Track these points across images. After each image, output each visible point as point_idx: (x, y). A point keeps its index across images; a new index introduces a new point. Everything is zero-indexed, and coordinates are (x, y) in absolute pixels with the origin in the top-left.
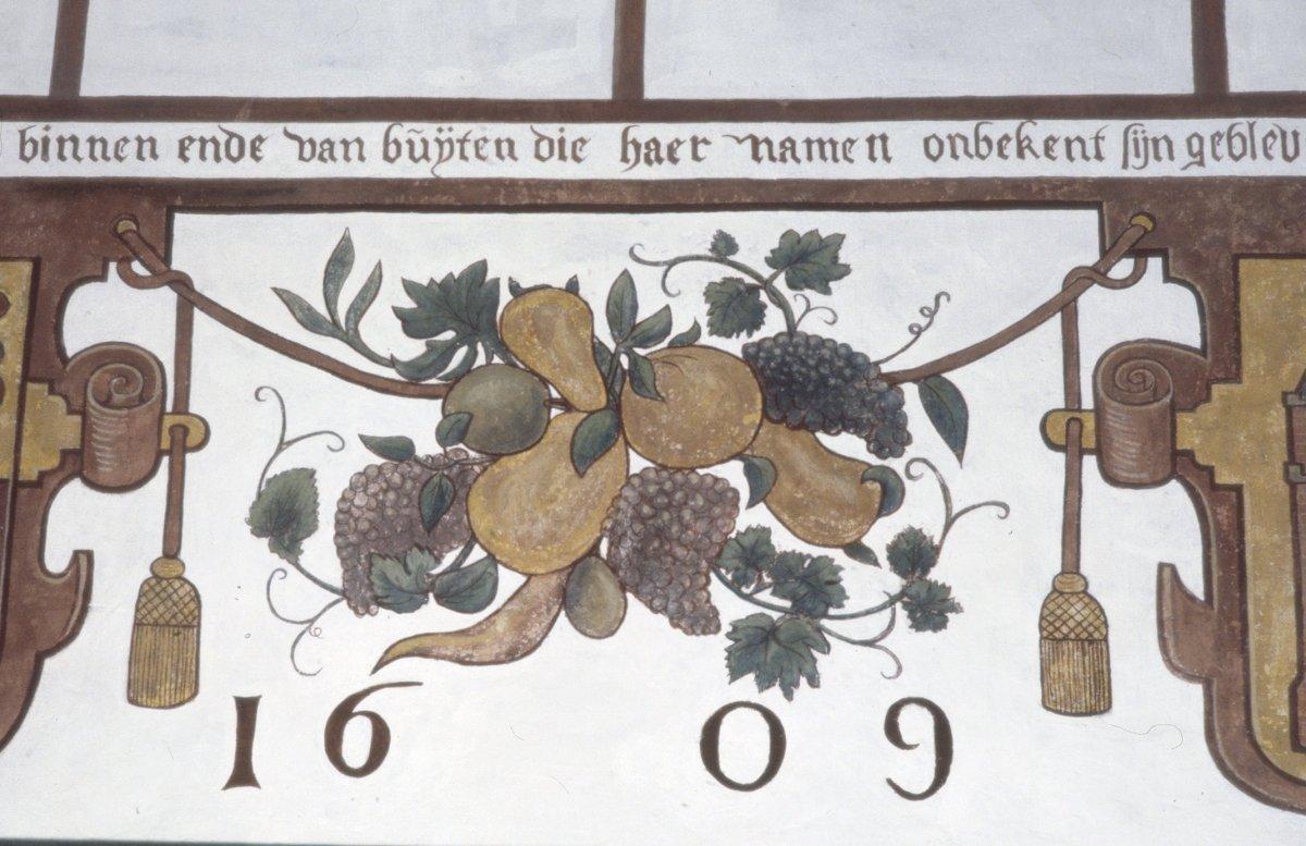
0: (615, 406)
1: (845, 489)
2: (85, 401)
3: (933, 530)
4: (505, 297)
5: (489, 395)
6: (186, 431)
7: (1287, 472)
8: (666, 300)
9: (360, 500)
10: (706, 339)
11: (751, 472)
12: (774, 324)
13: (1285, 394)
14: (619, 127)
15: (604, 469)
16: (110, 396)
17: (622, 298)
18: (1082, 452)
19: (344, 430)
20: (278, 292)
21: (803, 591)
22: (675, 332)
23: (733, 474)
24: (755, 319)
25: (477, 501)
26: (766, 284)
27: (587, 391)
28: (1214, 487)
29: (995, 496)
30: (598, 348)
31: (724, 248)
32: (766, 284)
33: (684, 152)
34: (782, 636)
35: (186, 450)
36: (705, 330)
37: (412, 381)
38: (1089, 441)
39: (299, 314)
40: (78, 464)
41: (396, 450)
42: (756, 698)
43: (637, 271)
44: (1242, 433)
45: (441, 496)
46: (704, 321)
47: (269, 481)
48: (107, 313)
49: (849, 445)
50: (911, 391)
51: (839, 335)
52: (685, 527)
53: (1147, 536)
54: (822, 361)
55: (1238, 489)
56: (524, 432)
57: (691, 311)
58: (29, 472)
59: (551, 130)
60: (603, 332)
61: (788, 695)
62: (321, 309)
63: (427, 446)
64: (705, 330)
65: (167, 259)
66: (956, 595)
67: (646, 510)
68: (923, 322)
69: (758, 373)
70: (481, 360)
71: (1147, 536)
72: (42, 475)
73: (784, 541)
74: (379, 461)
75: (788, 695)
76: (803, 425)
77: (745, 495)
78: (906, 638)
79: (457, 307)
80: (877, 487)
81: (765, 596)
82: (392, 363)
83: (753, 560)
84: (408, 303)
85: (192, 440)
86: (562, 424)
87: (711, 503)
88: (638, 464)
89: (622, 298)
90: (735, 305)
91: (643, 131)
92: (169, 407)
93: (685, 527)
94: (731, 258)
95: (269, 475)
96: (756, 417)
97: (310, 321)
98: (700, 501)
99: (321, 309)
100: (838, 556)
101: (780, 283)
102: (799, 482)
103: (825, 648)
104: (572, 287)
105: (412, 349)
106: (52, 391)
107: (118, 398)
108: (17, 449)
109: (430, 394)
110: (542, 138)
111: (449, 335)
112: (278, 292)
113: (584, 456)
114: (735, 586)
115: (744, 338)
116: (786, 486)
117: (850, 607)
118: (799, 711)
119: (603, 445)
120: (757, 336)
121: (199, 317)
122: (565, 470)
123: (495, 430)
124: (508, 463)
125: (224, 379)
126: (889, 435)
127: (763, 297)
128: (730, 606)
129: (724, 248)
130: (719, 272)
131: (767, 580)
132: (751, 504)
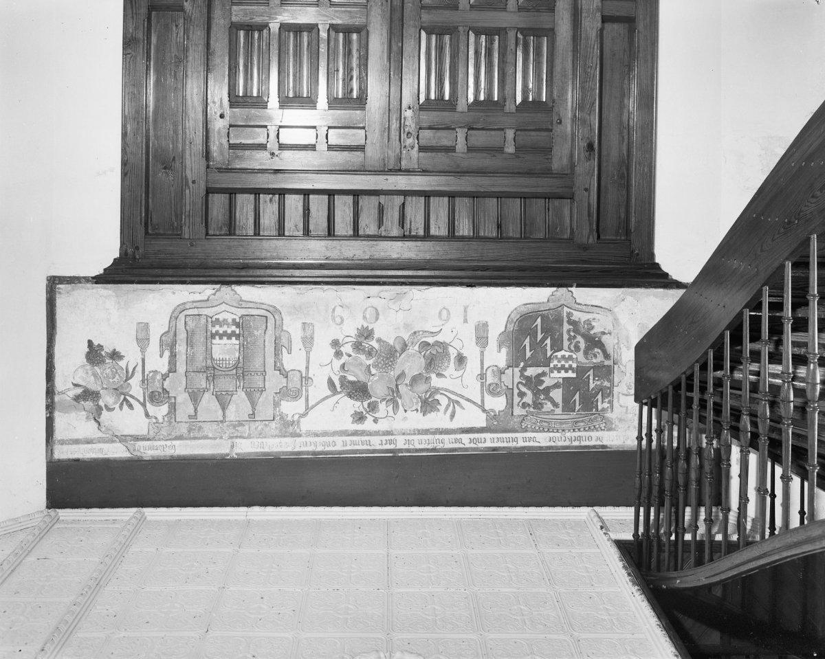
38: (304, 380)
44: (274, 381)
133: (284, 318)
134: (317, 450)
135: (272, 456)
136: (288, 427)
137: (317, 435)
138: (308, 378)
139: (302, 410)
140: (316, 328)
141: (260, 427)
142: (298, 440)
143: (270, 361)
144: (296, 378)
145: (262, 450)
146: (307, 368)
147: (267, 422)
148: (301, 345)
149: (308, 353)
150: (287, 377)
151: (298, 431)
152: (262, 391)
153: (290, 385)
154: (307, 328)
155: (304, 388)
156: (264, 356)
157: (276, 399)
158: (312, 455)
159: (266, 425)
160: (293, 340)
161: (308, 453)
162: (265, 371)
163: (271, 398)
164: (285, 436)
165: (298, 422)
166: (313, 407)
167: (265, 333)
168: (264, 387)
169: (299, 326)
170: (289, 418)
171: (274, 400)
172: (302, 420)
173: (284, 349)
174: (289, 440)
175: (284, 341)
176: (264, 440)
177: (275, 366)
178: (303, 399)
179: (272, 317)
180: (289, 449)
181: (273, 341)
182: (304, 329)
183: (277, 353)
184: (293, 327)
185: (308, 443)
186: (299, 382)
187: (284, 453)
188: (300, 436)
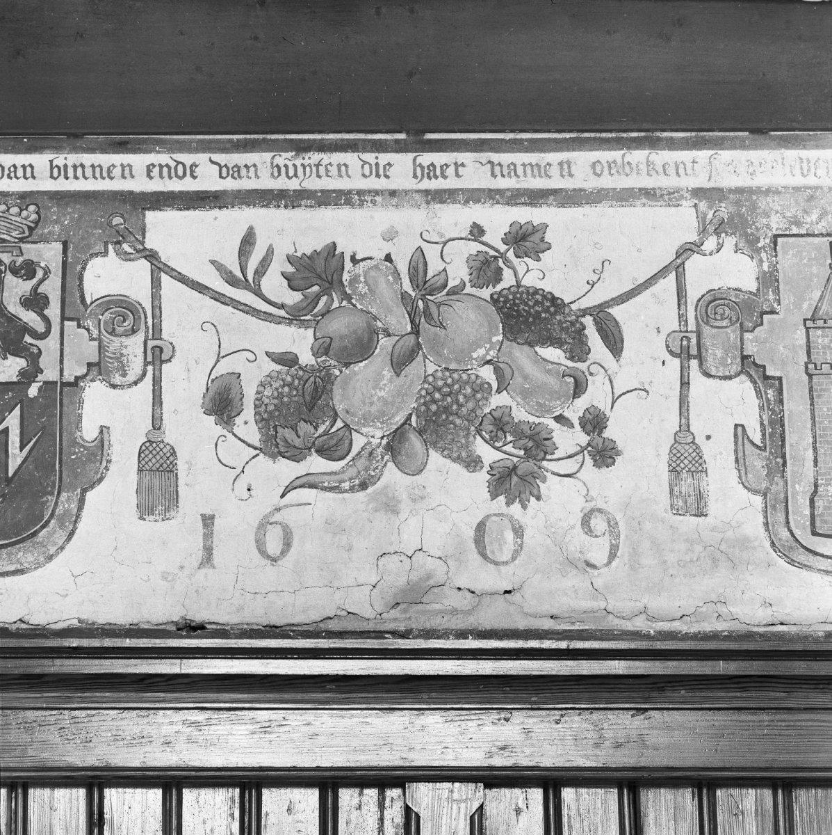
0: (416, 331)
1: (552, 381)
2: (100, 331)
3: (603, 404)
4: (348, 265)
5: (338, 326)
6: (161, 350)
7: (807, 368)
8: (444, 265)
9: (268, 392)
10: (468, 289)
11: (497, 371)
12: (508, 280)
13: (805, 320)
14: (411, 156)
15: (414, 369)
16: (114, 330)
17: (418, 267)
18: (689, 357)
19: (261, 347)
20: (213, 262)
21: (530, 444)
22: (451, 284)
23: (487, 374)
24: (498, 278)
25: (337, 392)
26: (503, 255)
27: (399, 321)
28: (766, 378)
29: (637, 384)
30: (404, 296)
31: (477, 232)
32: (503, 255)
33: (450, 171)
34: (520, 472)
35: (162, 362)
36: (468, 285)
37: (295, 316)
38: (694, 351)
39: (224, 276)
40: (97, 368)
41: (287, 360)
42: (504, 510)
43: (425, 246)
45: (316, 389)
46: (467, 279)
47: (213, 381)
48: (108, 276)
49: (553, 354)
50: (588, 321)
51: (547, 286)
52: (460, 406)
53: (727, 405)
54: (537, 303)
55: (780, 379)
56: (361, 348)
57: (459, 273)
58: (69, 377)
59: (369, 157)
60: (407, 286)
61: (524, 507)
62: (238, 274)
63: (306, 358)
64: (468, 285)
65: (142, 243)
66: (620, 445)
67: (437, 396)
68: (595, 278)
69: (499, 310)
70: (336, 304)
71: (727, 405)
72: (77, 378)
73: (520, 414)
74: (278, 367)
75: (524, 507)
76: (531, 344)
77: (495, 386)
78: (589, 471)
79: (320, 273)
80: (572, 380)
81: (509, 448)
82: (282, 306)
83: (500, 425)
84: (290, 269)
85: (164, 357)
86: (384, 343)
87: (475, 391)
88: (431, 368)
89: (418, 267)
90: (486, 269)
91: (426, 158)
92: (150, 337)
93: (460, 406)
94: (484, 239)
95: (213, 377)
96: (500, 338)
97: (232, 281)
98: (469, 390)
99: (238, 274)
100: (552, 424)
101: (510, 255)
102: (526, 377)
103: (544, 480)
104: (388, 258)
105: (293, 298)
106: (79, 326)
107: (119, 330)
108: (61, 362)
109: (303, 324)
110: (365, 162)
111: (316, 288)
112: (213, 262)
113: (399, 363)
114: (491, 442)
115: (490, 290)
116: (518, 379)
117: (558, 454)
118: (531, 515)
119: (411, 355)
120: (499, 288)
121: (165, 278)
122: (388, 373)
123: (346, 348)
124: (356, 368)
125: (183, 315)
126: (579, 350)
127: (501, 264)
128: (488, 454)
129: (477, 232)
130: (475, 247)
131: (509, 438)
132: (499, 391)
133: (762, 530)
134: (646, 152)
135: (773, 139)
136: (732, 216)
137: (649, 194)
138: (683, 354)
139: (694, 264)
140: (665, 500)
141: (814, 217)
142: (700, 181)
143: (795, 405)
144: (714, 354)
145: (804, 153)
146: (685, 384)
147: (795, 230)
148: (707, 449)
149: (685, 427)
150: (744, 358)
151: (703, 205)
152: (813, 319)
153: (732, 334)
154: (691, 500)
155: (692, 326)
156: (813, 418)
157: (771, 297)
158: (659, 139)
159: (798, 223)
160: (733, 464)
161: (672, 145)
162: (810, 376)
163: (787, 298)
164: (740, 191)
165: (703, 231)
166: (663, 273)
167: (816, 486)
168: (807, 329)
169: (713, 507)
170: (729, 242)
171: (777, 291)
172: (693, 237)
173: (757, 438)
174: (729, 181)
175: (757, 462)
176: (799, 181)
177: (780, 391)
178: (693, 294)
179: (797, 532)
180: (726, 155)
181: (789, 462)
182: (700, 497)
183: (776, 427)
184: (733, 502)
185: (671, 170)
186: (707, 341)
187: (743, 147)
188: (698, 193)
